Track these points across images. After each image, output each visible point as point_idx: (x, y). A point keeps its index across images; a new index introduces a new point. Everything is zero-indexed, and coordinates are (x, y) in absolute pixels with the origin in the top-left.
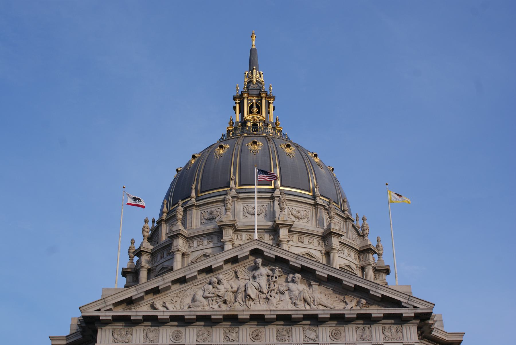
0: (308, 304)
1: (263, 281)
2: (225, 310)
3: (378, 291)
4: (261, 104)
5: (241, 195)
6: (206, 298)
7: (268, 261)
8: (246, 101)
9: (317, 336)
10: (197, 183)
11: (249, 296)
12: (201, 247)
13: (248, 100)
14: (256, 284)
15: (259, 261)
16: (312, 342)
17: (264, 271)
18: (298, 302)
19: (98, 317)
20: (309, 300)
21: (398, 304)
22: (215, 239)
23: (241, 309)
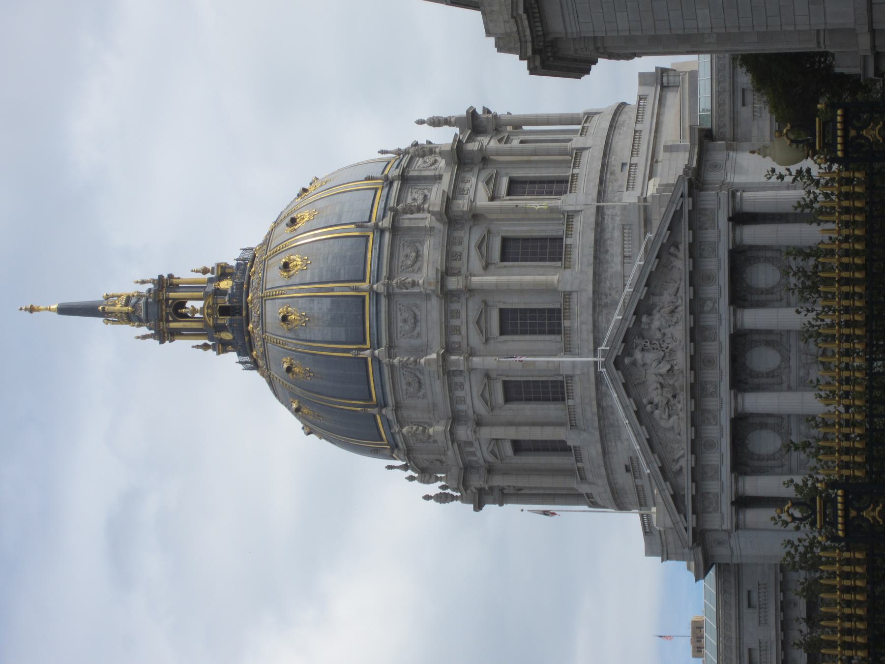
0: (676, 308)
1: (650, 357)
2: (683, 396)
3: (663, 235)
4: (174, 299)
5: (384, 342)
6: (670, 416)
7: (628, 351)
8: (173, 325)
9: (710, 299)
10: (354, 405)
11: (668, 371)
12: (468, 400)
13: (168, 321)
14: (655, 364)
15: (627, 360)
16: (717, 305)
17: (638, 355)
18: (675, 319)
19: (693, 529)
20: (672, 307)
21: (677, 216)
22: (458, 379)
23: (683, 379)
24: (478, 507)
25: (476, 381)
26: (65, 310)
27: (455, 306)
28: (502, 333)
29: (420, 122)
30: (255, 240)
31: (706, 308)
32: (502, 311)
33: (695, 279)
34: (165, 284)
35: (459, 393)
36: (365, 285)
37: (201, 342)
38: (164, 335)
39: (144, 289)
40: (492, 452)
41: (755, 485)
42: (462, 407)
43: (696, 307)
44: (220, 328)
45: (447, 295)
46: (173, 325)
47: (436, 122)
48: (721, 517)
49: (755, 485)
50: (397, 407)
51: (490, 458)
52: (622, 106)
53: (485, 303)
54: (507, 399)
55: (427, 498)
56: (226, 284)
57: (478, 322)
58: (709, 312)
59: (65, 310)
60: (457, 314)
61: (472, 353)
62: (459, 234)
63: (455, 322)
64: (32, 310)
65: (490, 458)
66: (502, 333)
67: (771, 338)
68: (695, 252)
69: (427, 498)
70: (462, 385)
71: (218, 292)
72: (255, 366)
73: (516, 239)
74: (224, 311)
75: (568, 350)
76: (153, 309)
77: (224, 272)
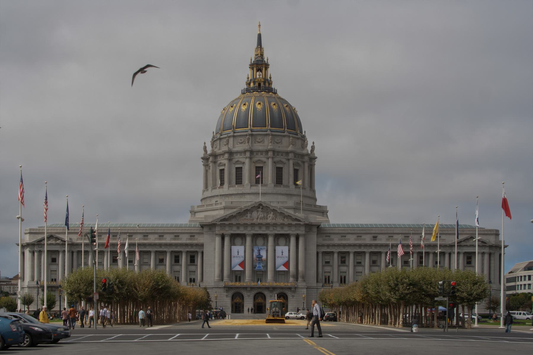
8: (255, 69)
21: (299, 221)
22: (243, 154)
24: (202, 158)
25: (242, 160)
26: (260, 36)
27: (264, 154)
28: (256, 167)
29: (313, 143)
30: (280, 94)
32: (262, 167)
33: (282, 225)
34: (267, 66)
35: (239, 155)
36: (269, 127)
37: (250, 77)
38: (252, 66)
39: (266, 60)
40: (221, 163)
41: (227, 240)
42: (235, 155)
43: (275, 225)
44: (254, 83)
45: (267, 152)
46: (255, 69)
47: (313, 148)
48: (218, 230)
49: (227, 240)
50: (234, 136)
51: (219, 162)
52: (316, 200)
53: (265, 162)
54: (237, 168)
55: (205, 143)
56: (267, 84)
57: (259, 160)
59: (260, 36)
60: (262, 154)
61: (251, 158)
62: (284, 155)
63: (259, 154)
65: (219, 162)
66: (256, 167)
67: (266, 244)
68: (290, 225)
69: (205, 143)
70: (241, 155)
71: (264, 83)
72: (243, 93)
73: (282, 171)
74: (259, 84)
75: (251, 186)
76: (260, 63)
77: (270, 83)
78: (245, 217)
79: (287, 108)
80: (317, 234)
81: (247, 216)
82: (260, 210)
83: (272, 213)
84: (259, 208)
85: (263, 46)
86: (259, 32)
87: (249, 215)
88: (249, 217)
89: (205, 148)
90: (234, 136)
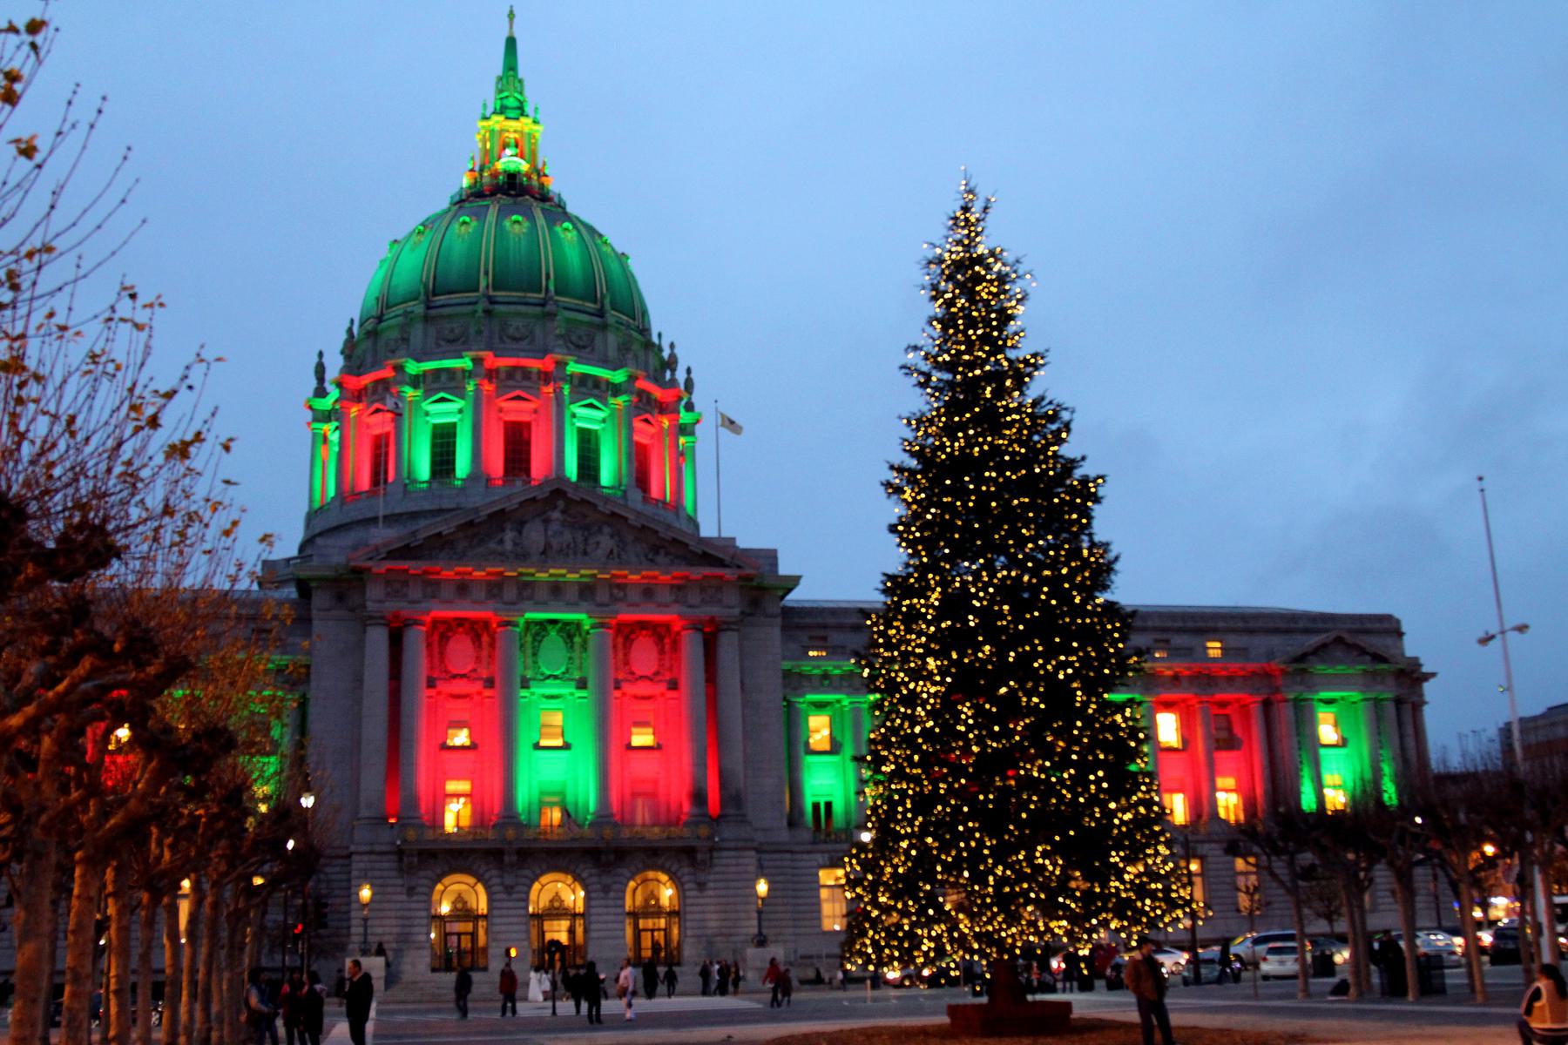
19: (369, 569)
21: (720, 563)
26: (511, 43)
31: (615, 591)
41: (415, 640)
55: (321, 354)
58: (611, 595)
59: (511, 43)
64: (511, 15)
69: (321, 354)
78: (492, 545)
79: (604, 249)
80: (784, 629)
81: (501, 541)
82: (556, 515)
83: (606, 530)
84: (555, 508)
85: (520, 75)
86: (506, 34)
87: (509, 536)
88: (508, 546)
89: (320, 371)
90: (426, 319)
